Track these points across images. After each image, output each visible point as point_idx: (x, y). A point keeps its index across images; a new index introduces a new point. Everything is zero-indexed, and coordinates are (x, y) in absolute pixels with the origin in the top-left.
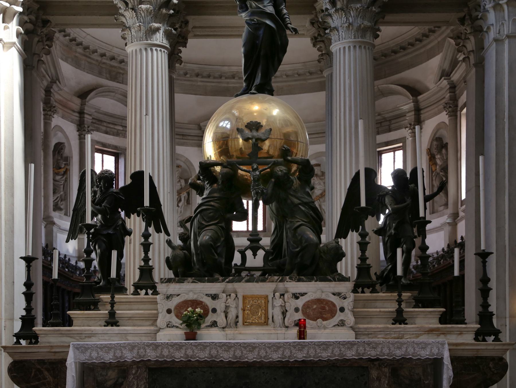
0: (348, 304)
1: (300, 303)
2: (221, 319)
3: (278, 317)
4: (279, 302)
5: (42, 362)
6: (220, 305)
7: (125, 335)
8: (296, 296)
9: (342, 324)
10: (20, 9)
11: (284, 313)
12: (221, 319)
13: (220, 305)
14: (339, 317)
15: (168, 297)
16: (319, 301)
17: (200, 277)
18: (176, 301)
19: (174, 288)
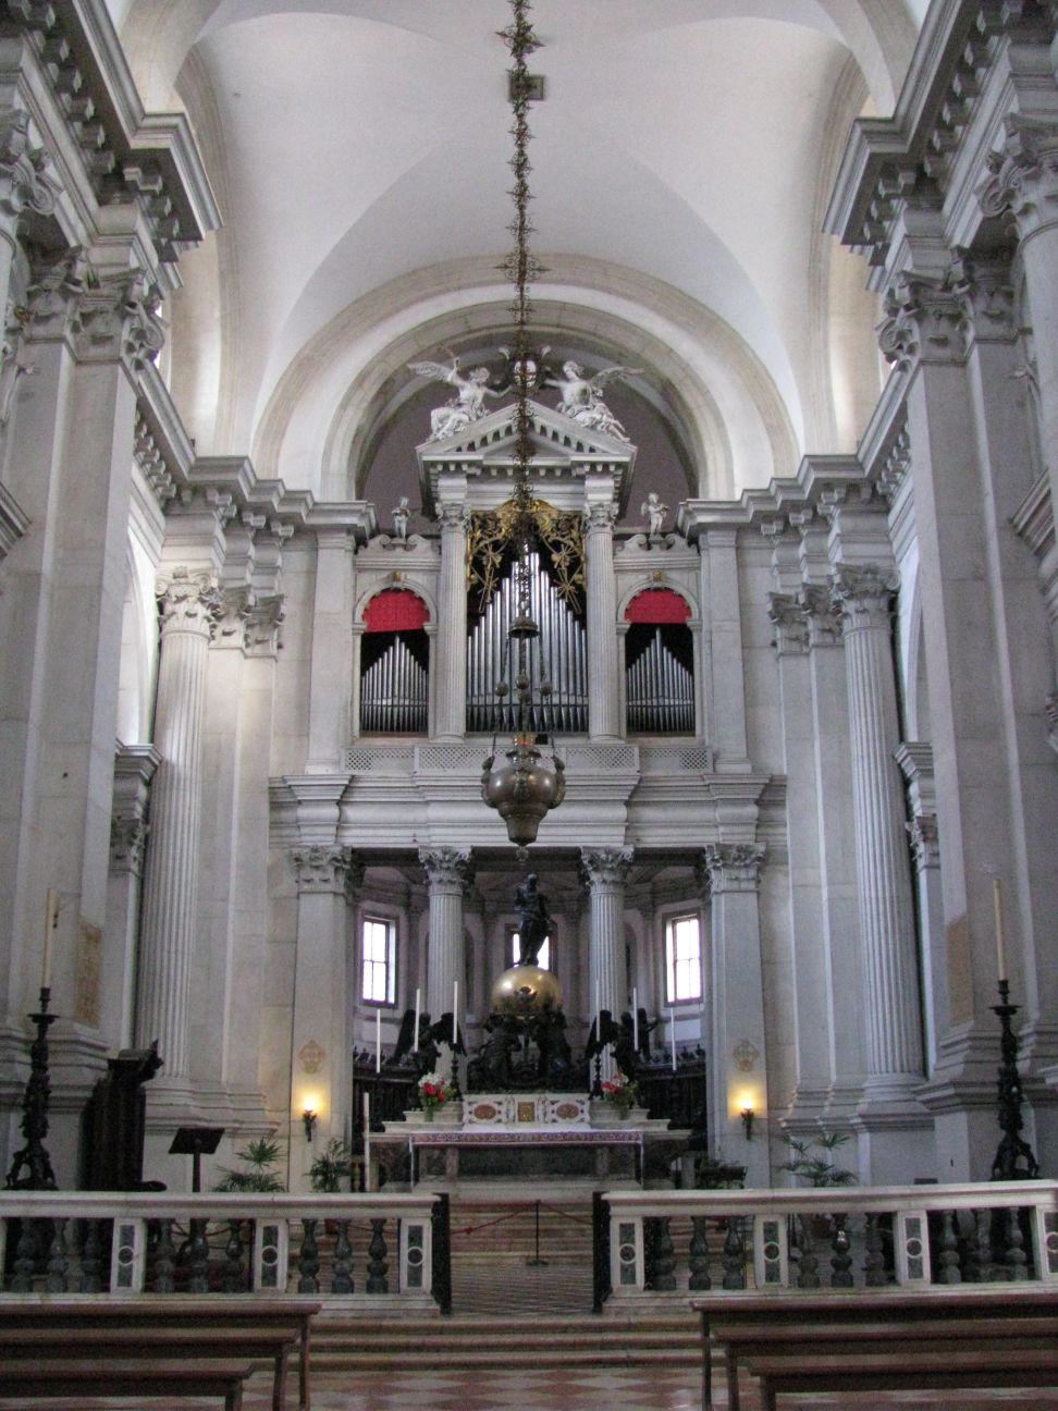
0: (586, 1107)
1: (555, 1107)
2: (503, 1117)
3: (541, 1117)
4: (541, 1107)
5: (387, 1144)
6: (503, 1109)
7: (440, 1127)
8: (553, 1103)
9: (582, 1120)
10: (347, 867)
11: (545, 1115)
12: (503, 1117)
13: (503, 1109)
14: (580, 1116)
15: (470, 1104)
16: (567, 1106)
17: (490, 1091)
18: (475, 1106)
19: (473, 1097)
